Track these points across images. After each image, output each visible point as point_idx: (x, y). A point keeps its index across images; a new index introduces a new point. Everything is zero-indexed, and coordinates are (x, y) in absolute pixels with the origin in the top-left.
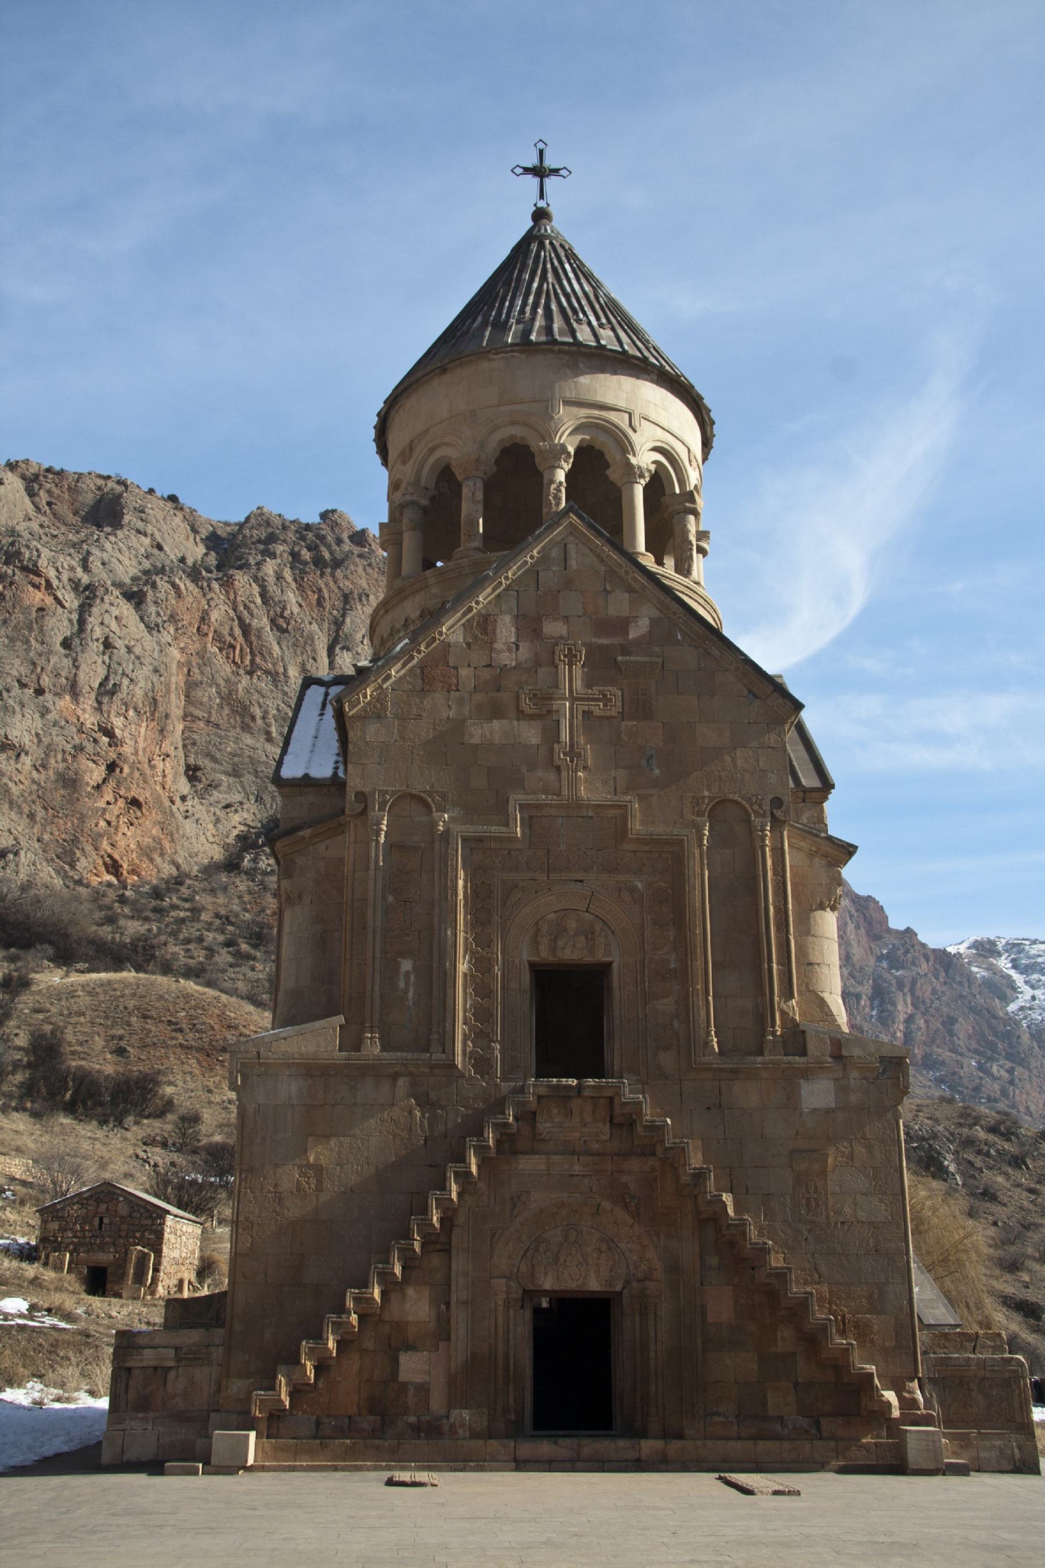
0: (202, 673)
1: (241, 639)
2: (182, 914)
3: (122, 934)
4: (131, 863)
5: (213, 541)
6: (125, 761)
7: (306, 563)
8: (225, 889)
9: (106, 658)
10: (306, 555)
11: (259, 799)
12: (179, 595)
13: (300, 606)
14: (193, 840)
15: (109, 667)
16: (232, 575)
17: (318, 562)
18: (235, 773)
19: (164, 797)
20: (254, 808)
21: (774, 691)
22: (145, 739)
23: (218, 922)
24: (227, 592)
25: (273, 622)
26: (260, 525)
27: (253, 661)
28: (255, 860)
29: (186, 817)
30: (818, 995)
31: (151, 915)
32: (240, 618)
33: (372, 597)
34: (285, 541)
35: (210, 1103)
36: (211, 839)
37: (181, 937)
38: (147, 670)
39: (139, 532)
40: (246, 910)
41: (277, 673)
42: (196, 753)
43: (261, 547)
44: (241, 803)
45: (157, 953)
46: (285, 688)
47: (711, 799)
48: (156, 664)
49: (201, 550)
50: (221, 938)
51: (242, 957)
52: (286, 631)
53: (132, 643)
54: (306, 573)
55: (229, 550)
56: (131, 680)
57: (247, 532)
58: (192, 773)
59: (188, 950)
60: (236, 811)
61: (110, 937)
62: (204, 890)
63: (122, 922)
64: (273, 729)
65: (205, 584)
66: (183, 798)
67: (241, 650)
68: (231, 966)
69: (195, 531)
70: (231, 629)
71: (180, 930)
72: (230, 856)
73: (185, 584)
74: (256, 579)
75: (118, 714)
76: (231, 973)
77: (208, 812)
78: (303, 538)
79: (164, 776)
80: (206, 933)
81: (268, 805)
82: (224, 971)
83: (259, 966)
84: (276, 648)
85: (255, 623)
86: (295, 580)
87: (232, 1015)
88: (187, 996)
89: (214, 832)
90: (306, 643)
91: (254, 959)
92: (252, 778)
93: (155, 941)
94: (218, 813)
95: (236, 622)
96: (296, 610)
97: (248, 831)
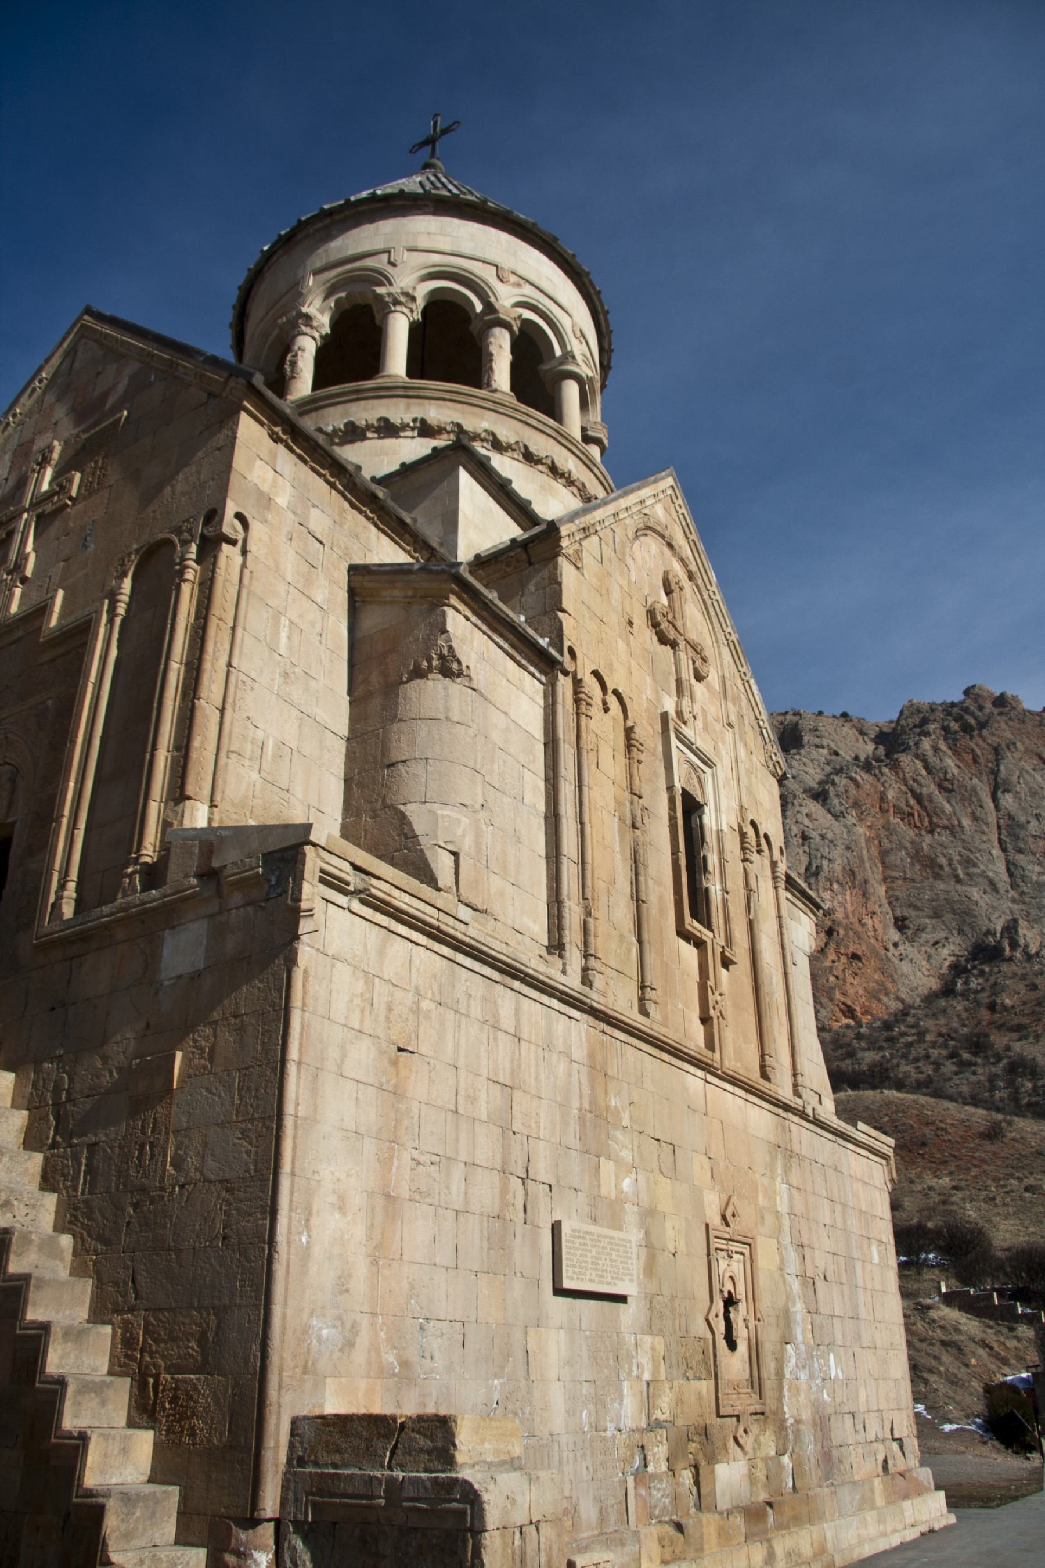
0: (891, 841)
1: (917, 807)
2: (910, 1039)
3: (859, 1064)
4: (863, 1006)
5: (881, 738)
6: (839, 924)
7: (956, 732)
8: (944, 1011)
9: (806, 848)
10: (955, 726)
11: (961, 932)
12: (857, 785)
13: (959, 767)
14: (912, 977)
15: (810, 854)
16: (897, 759)
17: (967, 729)
18: (936, 915)
19: (878, 946)
20: (958, 941)
21: (231, 375)
22: (852, 904)
23: (941, 1039)
24: (897, 773)
25: (940, 786)
26: (912, 714)
27: (931, 822)
28: (966, 983)
29: (901, 960)
30: (396, 809)
31: (884, 1044)
32: (912, 791)
33: (1018, 744)
34: (935, 720)
35: (913, 1191)
36: (927, 973)
37: (911, 1057)
38: (840, 849)
39: (817, 746)
40: (964, 1025)
41: (953, 826)
42: (901, 906)
43: (917, 730)
44: (946, 938)
45: (892, 1075)
46: (963, 837)
47: (137, 551)
48: (847, 842)
49: (870, 747)
50: (944, 1052)
51: (964, 1065)
52: (952, 790)
53: (824, 831)
54: (957, 740)
55: (892, 741)
56: (830, 860)
57: (903, 722)
58: (901, 923)
59: (918, 1068)
60: (944, 946)
61: (850, 1068)
62: (926, 1016)
63: (860, 1055)
64: (960, 872)
65: (877, 772)
66: (896, 945)
67: (919, 816)
68: (956, 1074)
69: (862, 733)
70: (907, 801)
71: (909, 1052)
72: (946, 984)
73: (861, 776)
74: (917, 756)
75: (825, 889)
76: (956, 1080)
77: (919, 952)
78: (949, 714)
79: (875, 930)
80: (931, 1051)
81: (970, 935)
82: (950, 1079)
83: (980, 1070)
84: (948, 808)
85: (925, 791)
86: (950, 748)
87: (929, 1113)
88: (888, 1103)
89: (928, 966)
90: (971, 796)
91: (975, 1064)
92: (951, 916)
93: (889, 1066)
94: (929, 950)
95: (910, 794)
96: (956, 771)
97: (958, 960)
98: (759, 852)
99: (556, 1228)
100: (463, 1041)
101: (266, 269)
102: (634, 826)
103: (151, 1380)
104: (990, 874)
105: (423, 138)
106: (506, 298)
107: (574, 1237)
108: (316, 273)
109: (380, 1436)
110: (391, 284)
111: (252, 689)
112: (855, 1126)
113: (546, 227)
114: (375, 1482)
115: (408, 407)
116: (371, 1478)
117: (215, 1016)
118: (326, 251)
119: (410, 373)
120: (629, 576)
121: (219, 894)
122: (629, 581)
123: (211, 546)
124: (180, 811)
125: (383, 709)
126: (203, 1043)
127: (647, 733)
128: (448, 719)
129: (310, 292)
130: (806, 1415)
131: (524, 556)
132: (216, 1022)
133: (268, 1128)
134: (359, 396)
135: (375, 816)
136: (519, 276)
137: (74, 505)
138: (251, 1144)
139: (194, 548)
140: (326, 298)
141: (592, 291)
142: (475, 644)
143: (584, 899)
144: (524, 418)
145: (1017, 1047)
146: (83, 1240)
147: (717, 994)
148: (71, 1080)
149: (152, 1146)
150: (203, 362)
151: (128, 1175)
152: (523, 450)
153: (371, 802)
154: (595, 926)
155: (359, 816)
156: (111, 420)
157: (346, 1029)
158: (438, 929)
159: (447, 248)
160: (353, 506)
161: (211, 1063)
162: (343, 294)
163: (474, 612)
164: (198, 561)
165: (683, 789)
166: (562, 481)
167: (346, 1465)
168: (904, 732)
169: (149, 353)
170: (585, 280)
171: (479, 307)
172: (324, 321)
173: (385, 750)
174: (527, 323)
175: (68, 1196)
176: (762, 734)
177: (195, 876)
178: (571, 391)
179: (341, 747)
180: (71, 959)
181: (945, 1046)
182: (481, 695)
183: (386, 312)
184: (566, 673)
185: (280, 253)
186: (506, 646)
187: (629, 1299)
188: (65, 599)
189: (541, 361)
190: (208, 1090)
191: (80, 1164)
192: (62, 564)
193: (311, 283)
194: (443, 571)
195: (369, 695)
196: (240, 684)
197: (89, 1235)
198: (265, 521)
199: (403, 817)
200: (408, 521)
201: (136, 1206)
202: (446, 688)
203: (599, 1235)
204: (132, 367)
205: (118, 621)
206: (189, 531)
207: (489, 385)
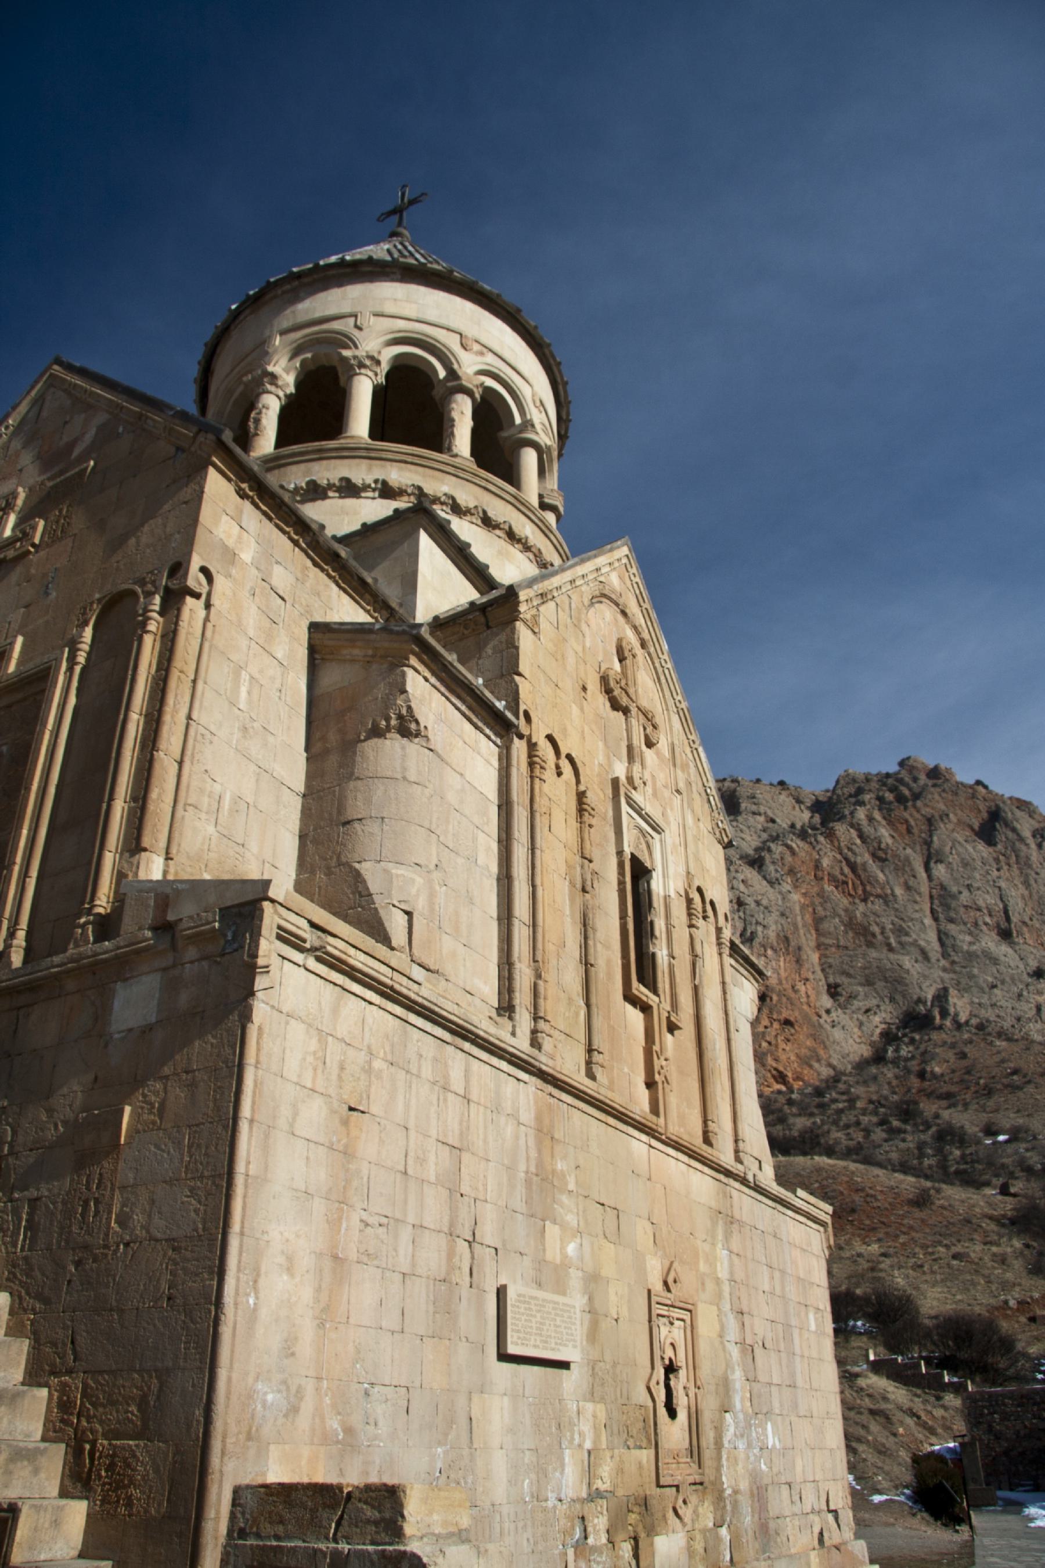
0: (825, 909)
1: (851, 875)
2: (841, 1106)
4: (795, 1072)
5: (817, 807)
6: (773, 990)
7: (891, 803)
8: (875, 1078)
9: (741, 914)
10: (889, 796)
11: (892, 1000)
12: (793, 853)
13: (893, 837)
14: (843, 1044)
15: (745, 920)
16: (832, 828)
17: (901, 799)
18: (869, 983)
19: (810, 1012)
20: (889, 1008)
21: (200, 430)
22: (785, 970)
23: (871, 1106)
24: (832, 841)
25: (874, 855)
26: (848, 783)
27: (864, 890)
28: (897, 1050)
29: (833, 1026)
30: (351, 867)
31: (816, 1111)
32: (847, 860)
33: (951, 816)
34: (870, 790)
35: (841, 1258)
36: (858, 1040)
37: (842, 1123)
38: (775, 915)
39: (754, 813)
40: (894, 1093)
41: (886, 895)
42: (834, 973)
43: (853, 800)
44: (878, 1006)
45: (822, 1141)
46: (896, 906)
47: (99, 601)
48: (781, 909)
49: (806, 815)
50: (875, 1119)
51: (893, 1132)
52: (885, 860)
53: (760, 897)
55: (827, 810)
56: (764, 926)
57: (839, 792)
58: (833, 990)
59: (848, 1134)
60: (875, 1013)
61: (781, 1134)
62: (858, 1083)
63: (791, 1120)
64: (892, 940)
65: (813, 840)
66: (828, 1012)
67: (853, 884)
68: (886, 1141)
69: (799, 801)
70: (841, 869)
71: (840, 1119)
72: (877, 1051)
73: (796, 843)
74: (852, 826)
76: (886, 1147)
77: (851, 1018)
79: (808, 997)
80: (861, 1117)
81: (901, 1003)
82: (880, 1146)
83: (909, 1138)
84: (881, 876)
85: (859, 860)
86: (884, 818)
87: (859, 1180)
88: (819, 1170)
89: (859, 1033)
90: (904, 865)
91: (905, 1132)
92: (883, 984)
93: (820, 1131)
94: (860, 1017)
95: (844, 863)
96: (890, 841)
97: (889, 1028)
98: (705, 918)
99: (501, 1293)
100: (413, 1102)
101: (232, 327)
102: (584, 890)
103: (87, 1447)
104: (922, 943)
105: (390, 207)
106: (469, 365)
107: (519, 1301)
108: (283, 333)
109: (325, 1506)
110: (356, 347)
111: (211, 742)
112: (794, 1192)
113: (510, 297)
114: (319, 1555)
115: (370, 469)
116: (315, 1551)
117: (167, 1070)
118: (294, 312)
119: (373, 434)
120: (584, 642)
121: (174, 947)
122: (584, 647)
123: (175, 597)
124: (135, 863)
125: (340, 767)
126: (153, 1098)
127: (599, 798)
128: (404, 778)
129: (276, 351)
130: (744, 1485)
131: (483, 620)
132: (167, 1077)
133: (217, 1186)
134: (322, 456)
135: (329, 873)
136: (481, 345)
137: (37, 552)
138: (200, 1202)
139: (157, 599)
140: (291, 359)
141: (552, 361)
142: (434, 705)
143: (535, 961)
144: (483, 483)
145: (946, 1114)
146: (20, 1297)
147: (662, 1058)
148: (14, 1133)
149: (97, 1202)
150: (173, 416)
151: (70, 1232)
152: (481, 515)
153: (326, 859)
154: (545, 989)
155: (313, 872)
156: (77, 470)
157: (298, 1087)
158: (392, 988)
159: (413, 315)
160: (315, 564)
161: (161, 1119)
162: (309, 355)
163: (433, 673)
164: (161, 613)
165: (632, 854)
166: (520, 546)
167: (289, 1537)
168: (839, 801)
169: (118, 405)
170: (546, 351)
171: (442, 374)
172: (289, 381)
173: (341, 808)
174: (488, 391)
175: (7, 1253)
176: (709, 801)
177: (149, 929)
178: (529, 459)
179: (297, 803)
180: (19, 1009)
181: (875, 1113)
182: (439, 756)
183: (351, 375)
184: (521, 736)
185: (248, 311)
186: (463, 708)
187: (572, 1365)
188: (24, 645)
189: (501, 428)
190: (157, 1146)
191: (20, 1220)
192: (23, 610)
193: (277, 342)
194: (404, 632)
195: (326, 752)
196: (199, 737)
197: (28, 1294)
198: (229, 576)
199: (358, 875)
200: (369, 580)
201: (78, 1264)
202: (403, 748)
203: (544, 1300)
204: (101, 418)
205: (78, 669)
206: (153, 583)
207: (450, 449)
